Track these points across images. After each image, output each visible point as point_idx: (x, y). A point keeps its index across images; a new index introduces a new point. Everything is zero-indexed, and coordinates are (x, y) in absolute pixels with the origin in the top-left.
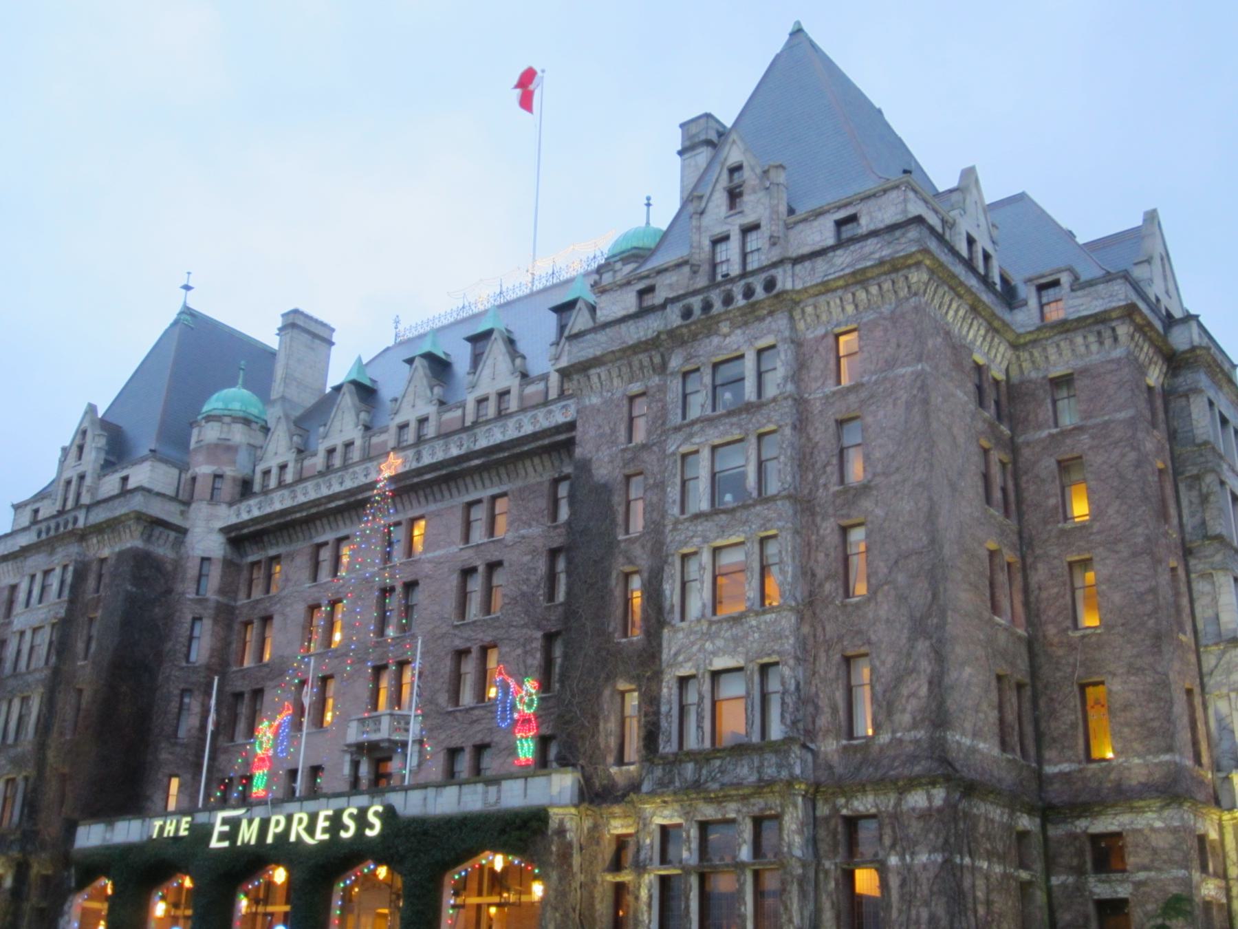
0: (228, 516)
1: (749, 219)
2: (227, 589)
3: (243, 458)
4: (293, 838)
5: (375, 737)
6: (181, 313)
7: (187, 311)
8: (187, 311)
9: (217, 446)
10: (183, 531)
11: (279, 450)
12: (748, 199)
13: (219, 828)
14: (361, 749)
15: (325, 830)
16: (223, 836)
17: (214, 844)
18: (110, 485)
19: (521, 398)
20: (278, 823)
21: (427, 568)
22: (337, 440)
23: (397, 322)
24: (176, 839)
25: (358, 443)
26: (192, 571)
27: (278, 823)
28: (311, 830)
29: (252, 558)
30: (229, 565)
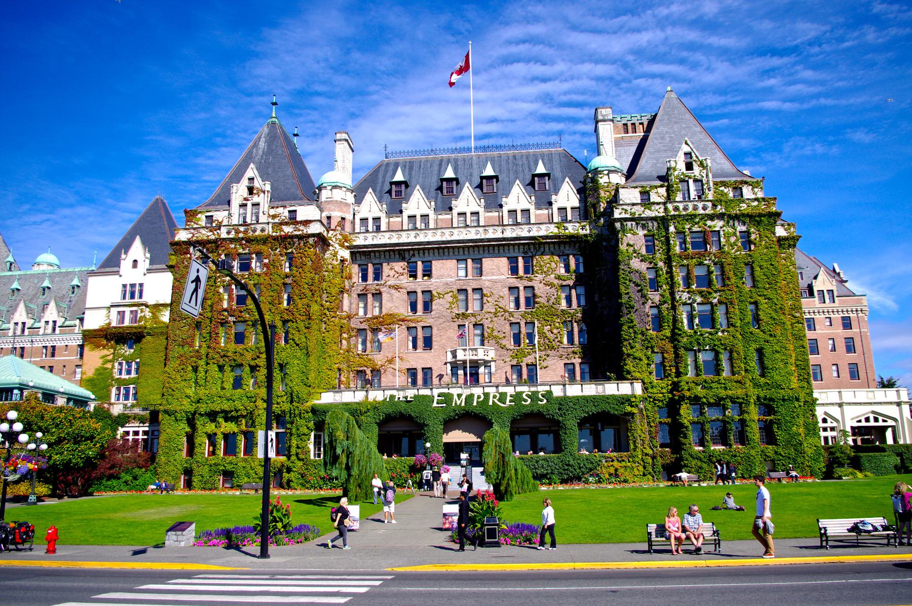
4: (491, 403)
9: (341, 202)
13: (436, 398)
17: (435, 404)
19: (536, 216)
21: (487, 283)
23: (386, 147)
24: (408, 402)
27: (479, 397)
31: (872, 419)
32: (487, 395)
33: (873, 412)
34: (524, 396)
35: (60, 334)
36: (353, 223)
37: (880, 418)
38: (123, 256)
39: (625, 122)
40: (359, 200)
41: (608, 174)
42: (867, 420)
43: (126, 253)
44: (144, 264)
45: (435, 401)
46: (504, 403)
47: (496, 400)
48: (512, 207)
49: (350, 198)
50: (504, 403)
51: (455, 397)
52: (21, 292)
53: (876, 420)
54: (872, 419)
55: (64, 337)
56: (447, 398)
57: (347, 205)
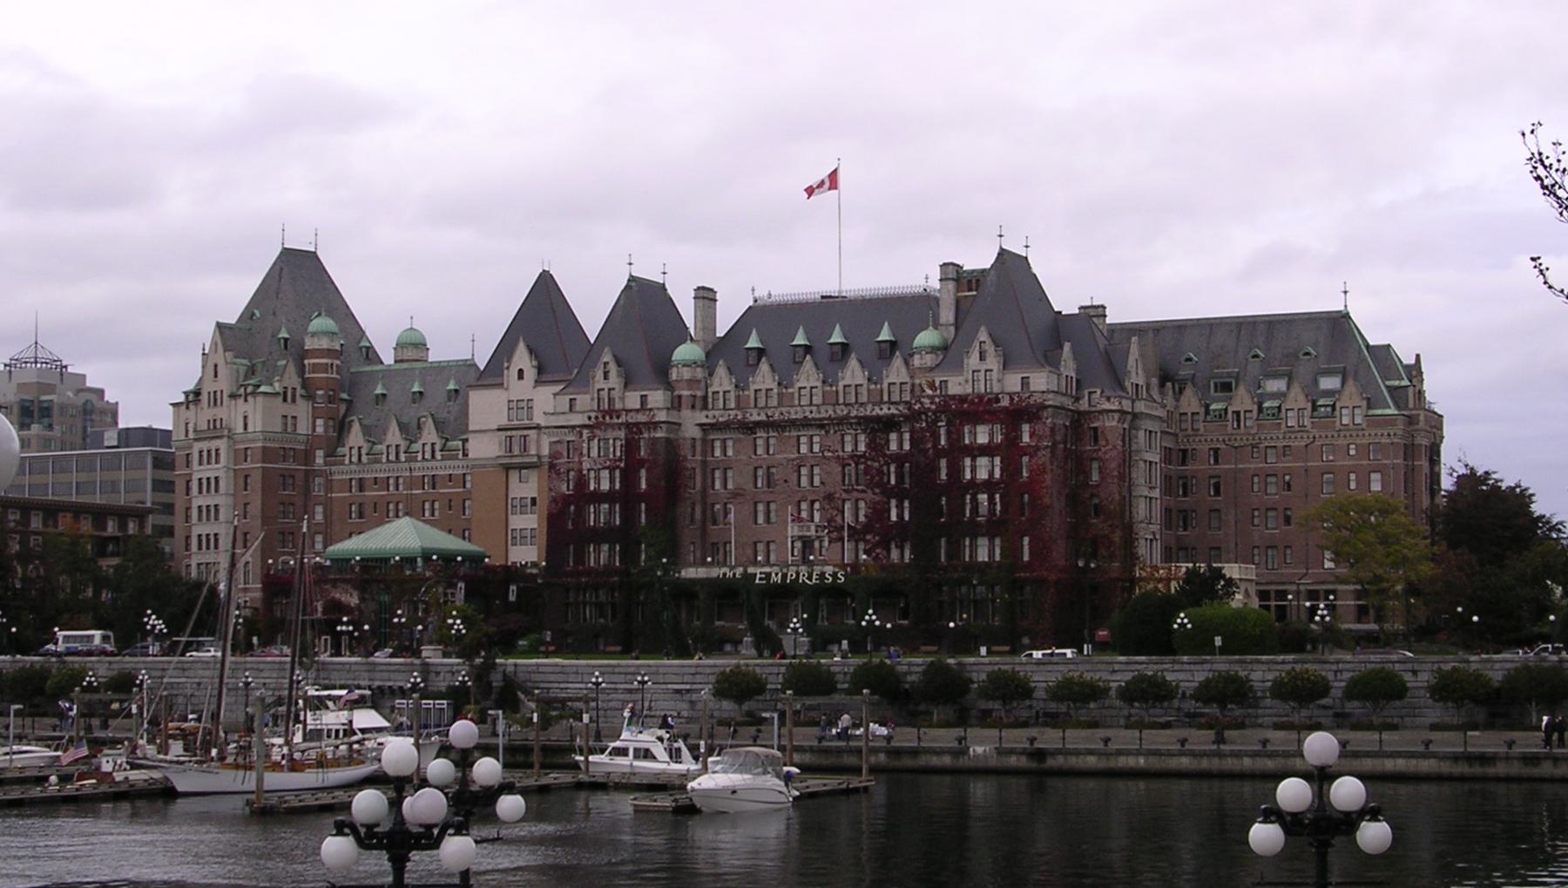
0: (701, 417)
1: (989, 367)
2: (704, 453)
3: (703, 384)
5: (808, 534)
6: (629, 280)
7: (632, 279)
8: (632, 279)
9: (691, 380)
10: (680, 424)
11: (722, 381)
12: (988, 360)
13: (758, 576)
14: (800, 538)
16: (760, 579)
17: (757, 581)
18: (633, 401)
19: (869, 390)
22: (764, 387)
23: (753, 290)
26: (688, 444)
28: (810, 578)
29: (712, 437)
30: (704, 440)
32: (798, 574)
34: (827, 576)
35: (442, 460)
36: (705, 398)
38: (506, 365)
43: (509, 361)
44: (531, 374)
46: (811, 580)
48: (846, 382)
49: (700, 373)
50: (811, 580)
51: (773, 575)
52: (388, 399)
55: (448, 463)
56: (768, 575)
57: (699, 381)
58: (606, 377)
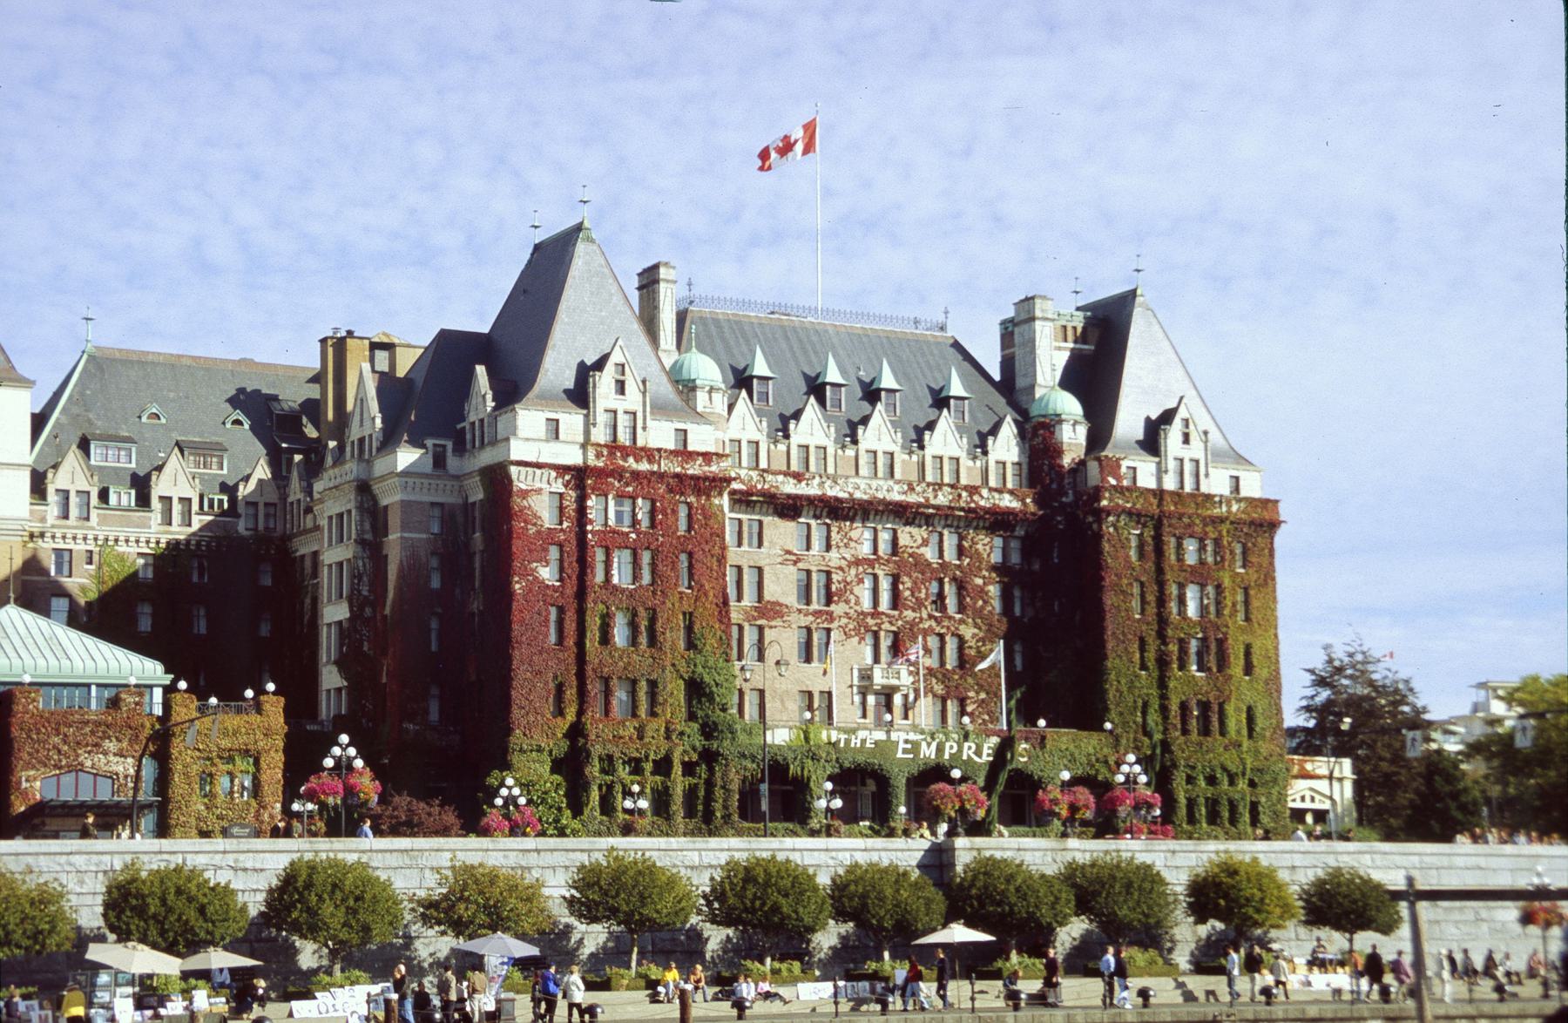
13: (902, 746)
15: (989, 755)
16: (905, 751)
17: (900, 755)
20: (951, 747)
25: (831, 451)
27: (951, 747)
31: (1308, 799)
33: (1312, 789)
37: (1317, 797)
39: (1064, 323)
40: (731, 407)
41: (1074, 425)
42: (1303, 799)
45: (900, 751)
46: (980, 757)
47: (971, 753)
50: (980, 757)
53: (1313, 799)
54: (1308, 799)
58: (621, 387)
